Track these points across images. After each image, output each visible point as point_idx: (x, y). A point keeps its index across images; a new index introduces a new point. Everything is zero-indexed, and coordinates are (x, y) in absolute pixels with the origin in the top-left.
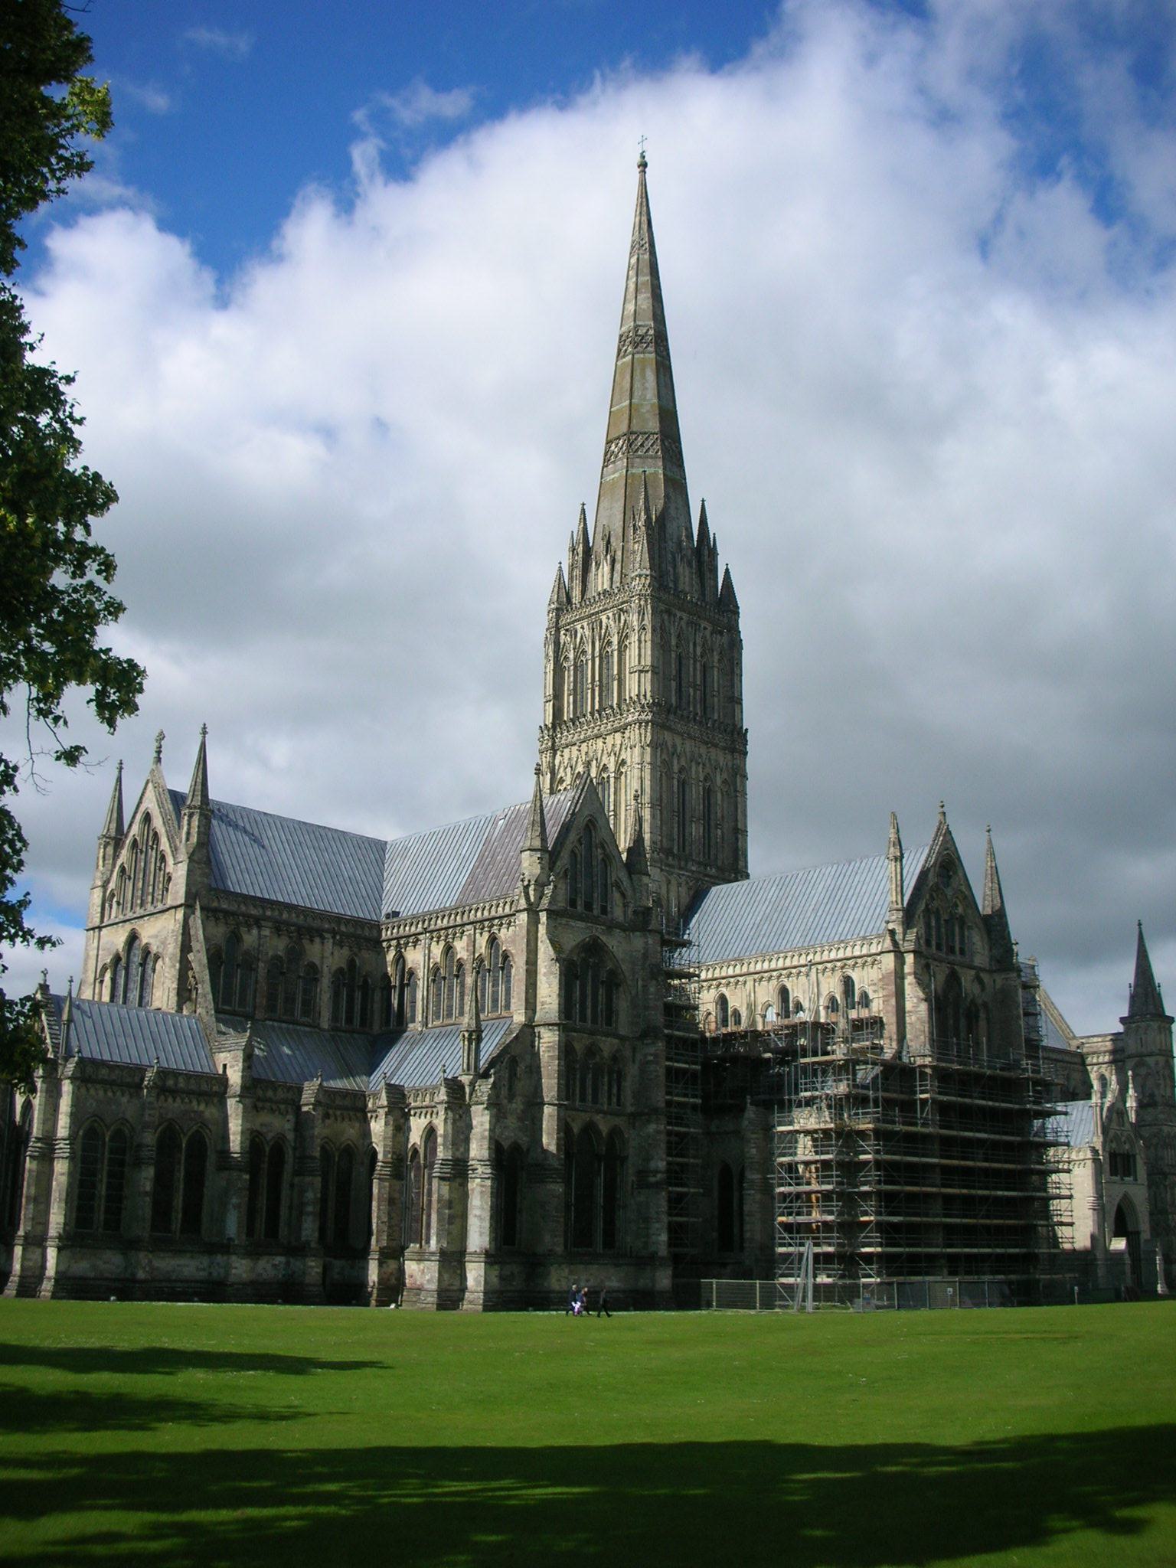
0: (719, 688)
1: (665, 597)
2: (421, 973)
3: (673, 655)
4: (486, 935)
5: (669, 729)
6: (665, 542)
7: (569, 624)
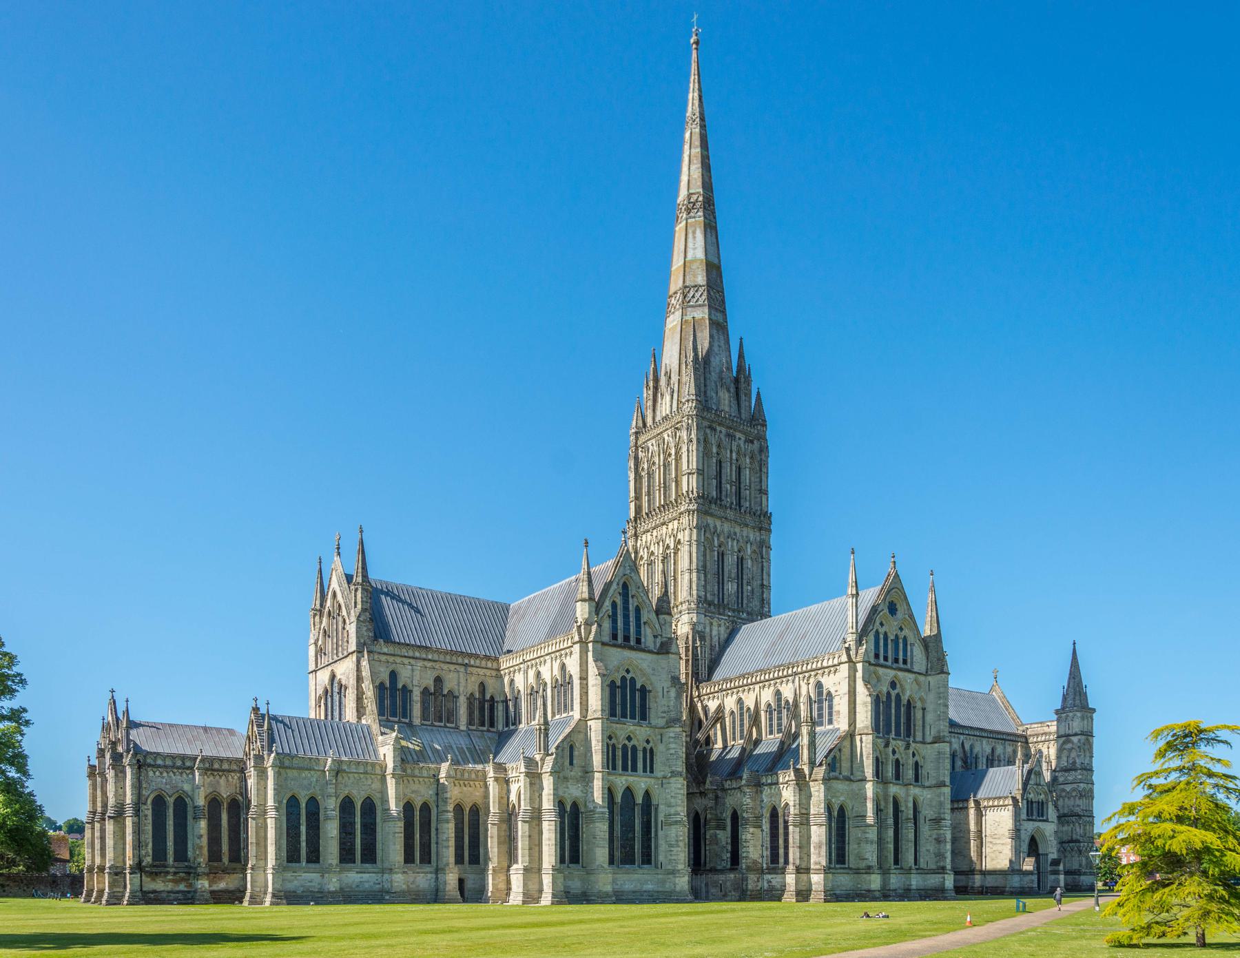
0: (750, 483)
3: (714, 460)
5: (712, 515)
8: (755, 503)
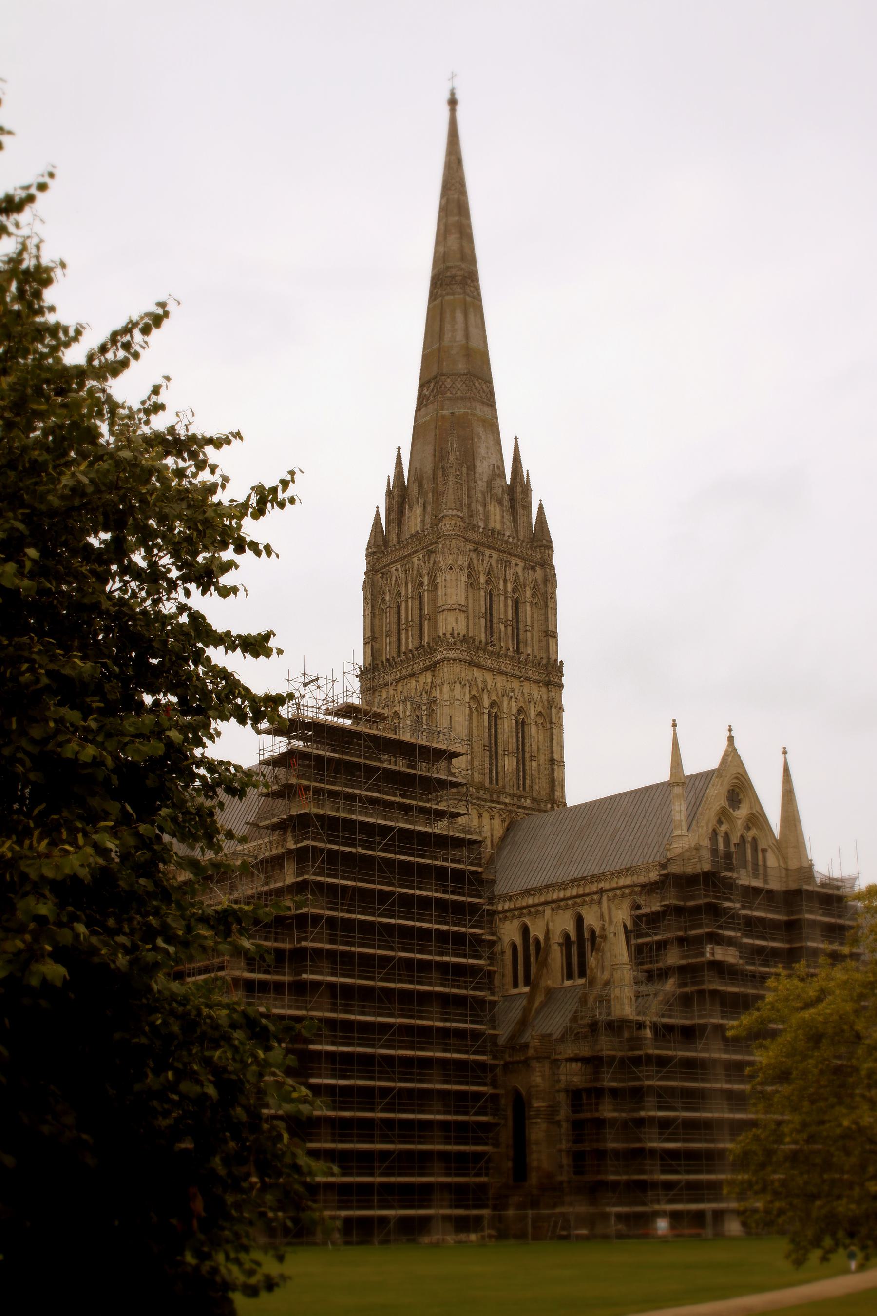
0: (532, 623)
1: (473, 536)
3: (482, 593)
5: (479, 666)
6: (475, 482)
7: (385, 566)
8: (540, 648)
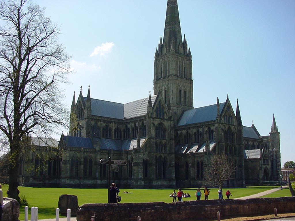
2: (131, 129)
4: (141, 122)
